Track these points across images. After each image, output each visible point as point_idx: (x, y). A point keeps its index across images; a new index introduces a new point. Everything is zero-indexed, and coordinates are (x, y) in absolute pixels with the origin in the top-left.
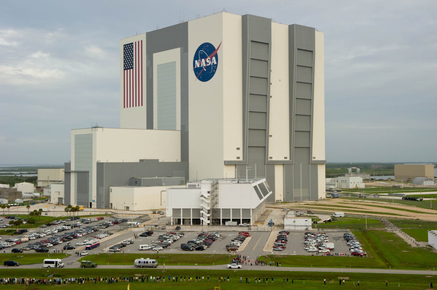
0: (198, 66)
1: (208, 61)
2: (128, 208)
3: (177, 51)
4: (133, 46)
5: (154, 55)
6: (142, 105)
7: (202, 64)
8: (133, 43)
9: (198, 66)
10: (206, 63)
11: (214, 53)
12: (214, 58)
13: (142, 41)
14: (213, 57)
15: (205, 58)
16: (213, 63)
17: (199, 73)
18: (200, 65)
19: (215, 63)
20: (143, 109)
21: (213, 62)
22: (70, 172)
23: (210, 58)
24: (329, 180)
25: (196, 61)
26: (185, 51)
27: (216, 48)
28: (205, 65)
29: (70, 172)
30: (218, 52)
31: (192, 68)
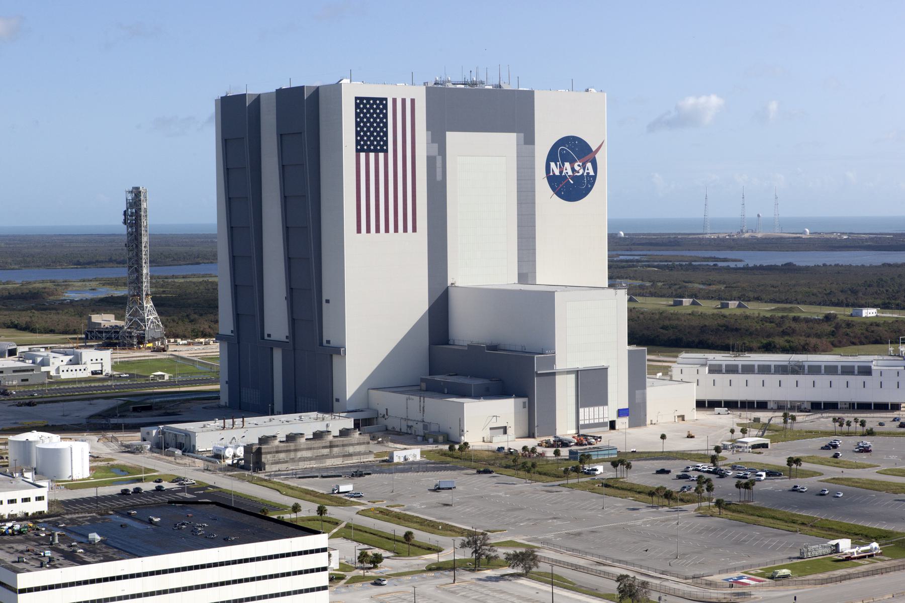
0: (557, 173)
1: (577, 168)
2: (682, 418)
4: (385, 107)
5: (449, 134)
6: (414, 230)
8: (386, 99)
9: (557, 173)
10: (573, 170)
11: (589, 156)
12: (589, 165)
13: (413, 101)
14: (587, 162)
15: (572, 162)
16: (588, 173)
17: (558, 185)
18: (561, 172)
19: (592, 173)
22: (554, 374)
24: (634, 348)
25: (553, 165)
27: (594, 149)
29: (554, 374)
30: (597, 156)
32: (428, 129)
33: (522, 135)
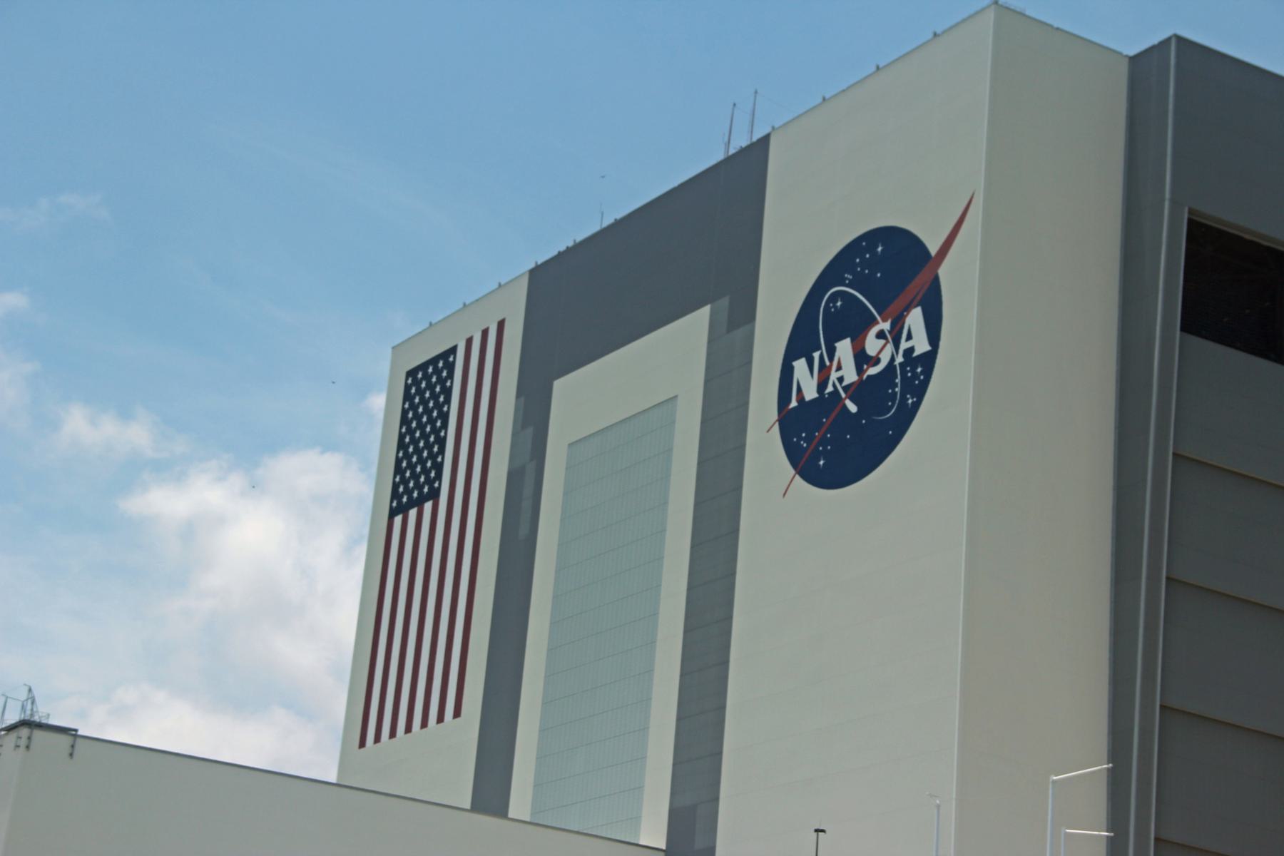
0: (810, 393)
1: (872, 345)
3: (695, 327)
4: (451, 367)
6: (457, 713)
7: (834, 376)
8: (453, 350)
10: (862, 359)
11: (919, 283)
12: (915, 319)
13: (501, 325)
14: (908, 309)
18: (822, 386)
19: (921, 345)
20: (462, 735)
21: (904, 345)
23: (886, 326)
25: (800, 365)
26: (740, 313)
27: (933, 249)
28: (851, 376)
30: (943, 272)
31: (773, 414)
32: (519, 395)
33: (725, 302)
